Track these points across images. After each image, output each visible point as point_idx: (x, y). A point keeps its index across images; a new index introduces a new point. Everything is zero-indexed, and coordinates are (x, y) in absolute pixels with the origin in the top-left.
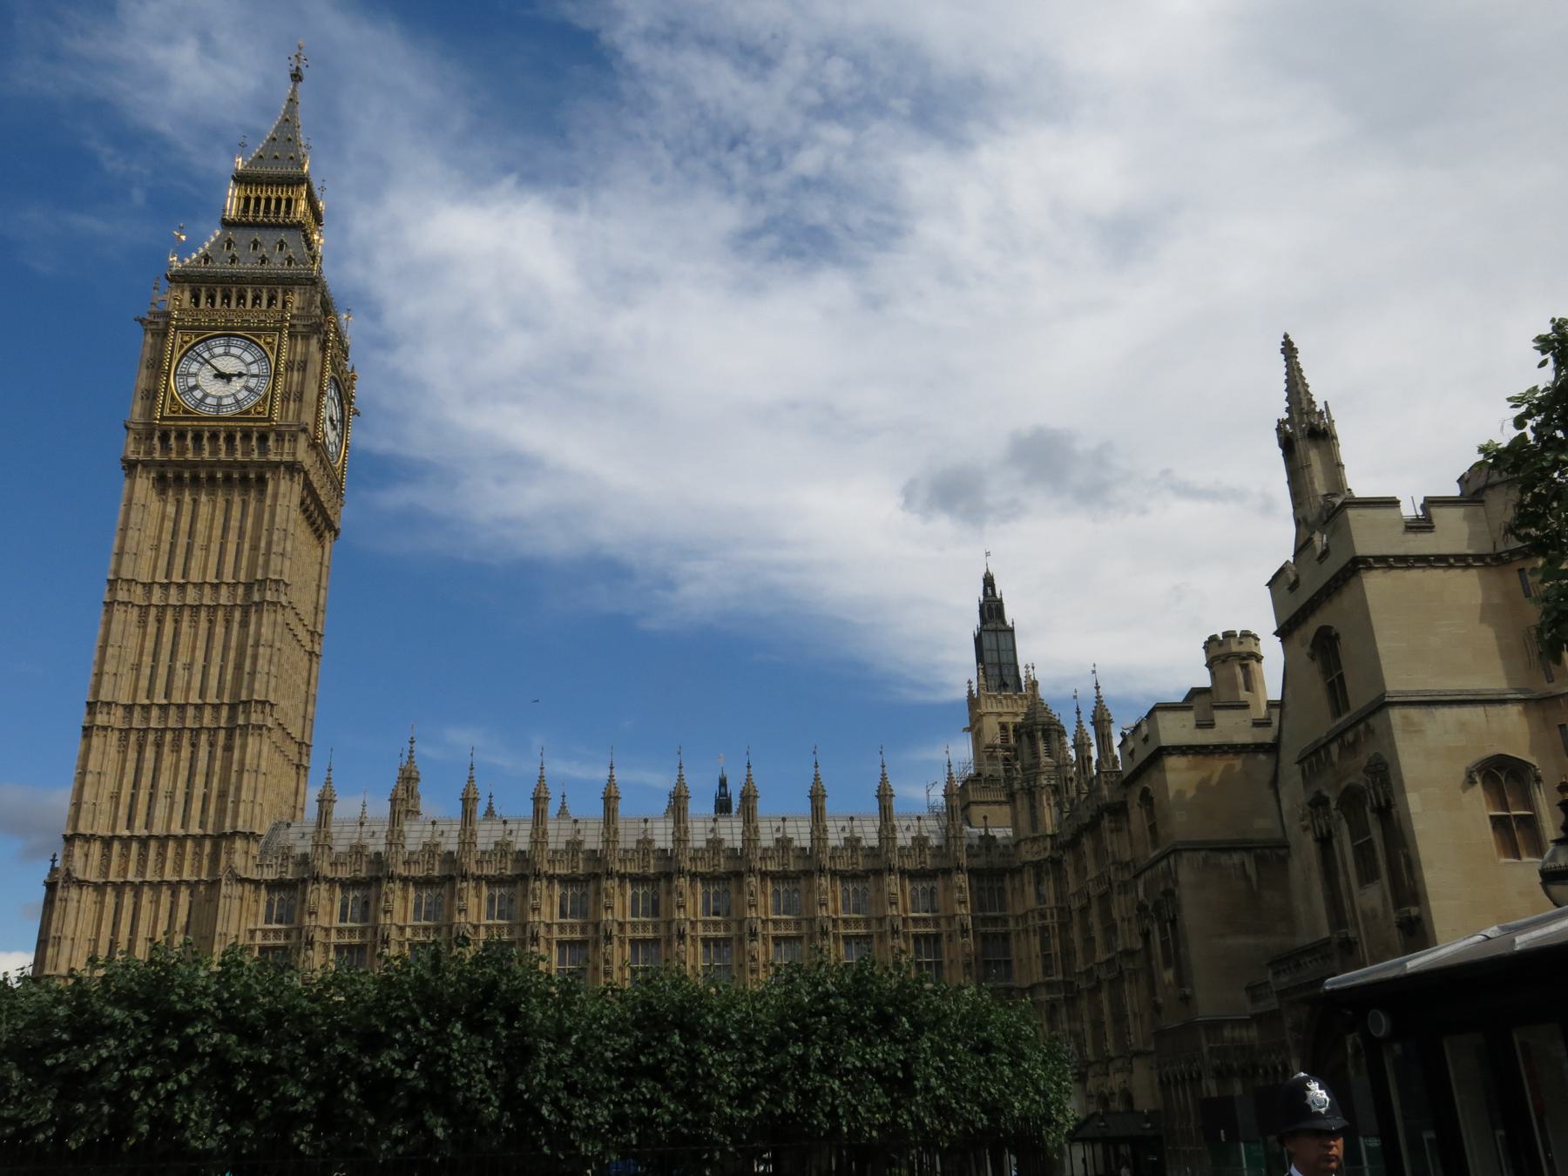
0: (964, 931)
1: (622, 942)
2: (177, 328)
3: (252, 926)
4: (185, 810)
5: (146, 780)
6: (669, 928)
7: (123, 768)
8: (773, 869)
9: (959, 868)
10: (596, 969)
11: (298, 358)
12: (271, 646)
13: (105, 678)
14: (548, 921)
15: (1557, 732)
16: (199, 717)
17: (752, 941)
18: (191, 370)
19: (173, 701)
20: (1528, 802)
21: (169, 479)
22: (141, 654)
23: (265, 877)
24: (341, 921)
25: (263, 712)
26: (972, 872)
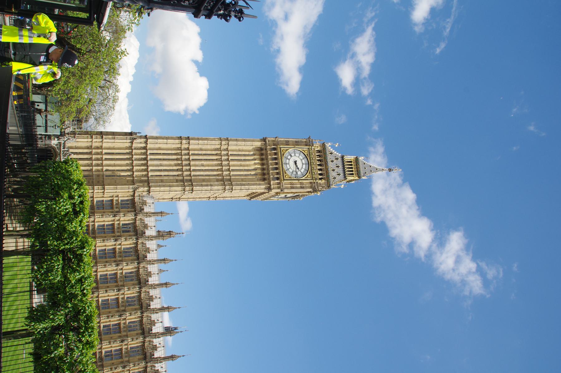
1: (119, 320)
2: (309, 148)
3: (119, 196)
8: (148, 370)
10: (110, 312)
16: (187, 170)
17: (122, 367)
18: (296, 154)
21: (261, 152)
23: (136, 198)
25: (189, 190)
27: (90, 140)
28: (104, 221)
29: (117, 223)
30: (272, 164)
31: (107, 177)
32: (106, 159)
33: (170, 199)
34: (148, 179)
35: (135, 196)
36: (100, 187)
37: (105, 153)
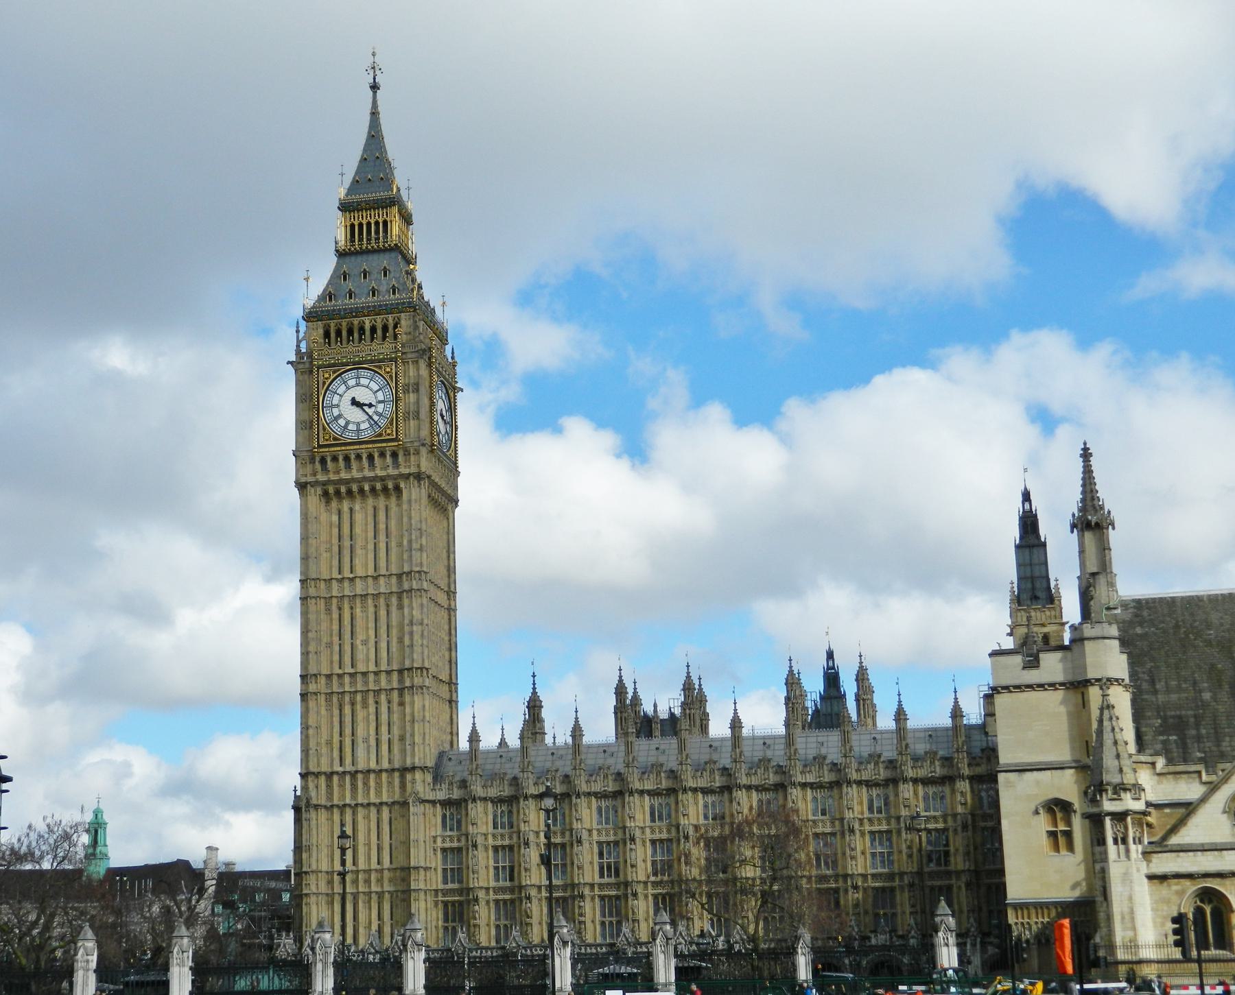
0: (965, 827)
2: (318, 369)
3: (433, 834)
4: (377, 751)
5: (348, 731)
7: (332, 722)
9: (962, 777)
12: (422, 624)
13: (311, 656)
14: (642, 825)
16: (377, 682)
18: (335, 402)
20: (1069, 823)
22: (331, 635)
23: (438, 798)
24: (494, 828)
26: (973, 779)
29: (491, 841)
30: (361, 469)
34: (398, 770)
36: (412, 878)
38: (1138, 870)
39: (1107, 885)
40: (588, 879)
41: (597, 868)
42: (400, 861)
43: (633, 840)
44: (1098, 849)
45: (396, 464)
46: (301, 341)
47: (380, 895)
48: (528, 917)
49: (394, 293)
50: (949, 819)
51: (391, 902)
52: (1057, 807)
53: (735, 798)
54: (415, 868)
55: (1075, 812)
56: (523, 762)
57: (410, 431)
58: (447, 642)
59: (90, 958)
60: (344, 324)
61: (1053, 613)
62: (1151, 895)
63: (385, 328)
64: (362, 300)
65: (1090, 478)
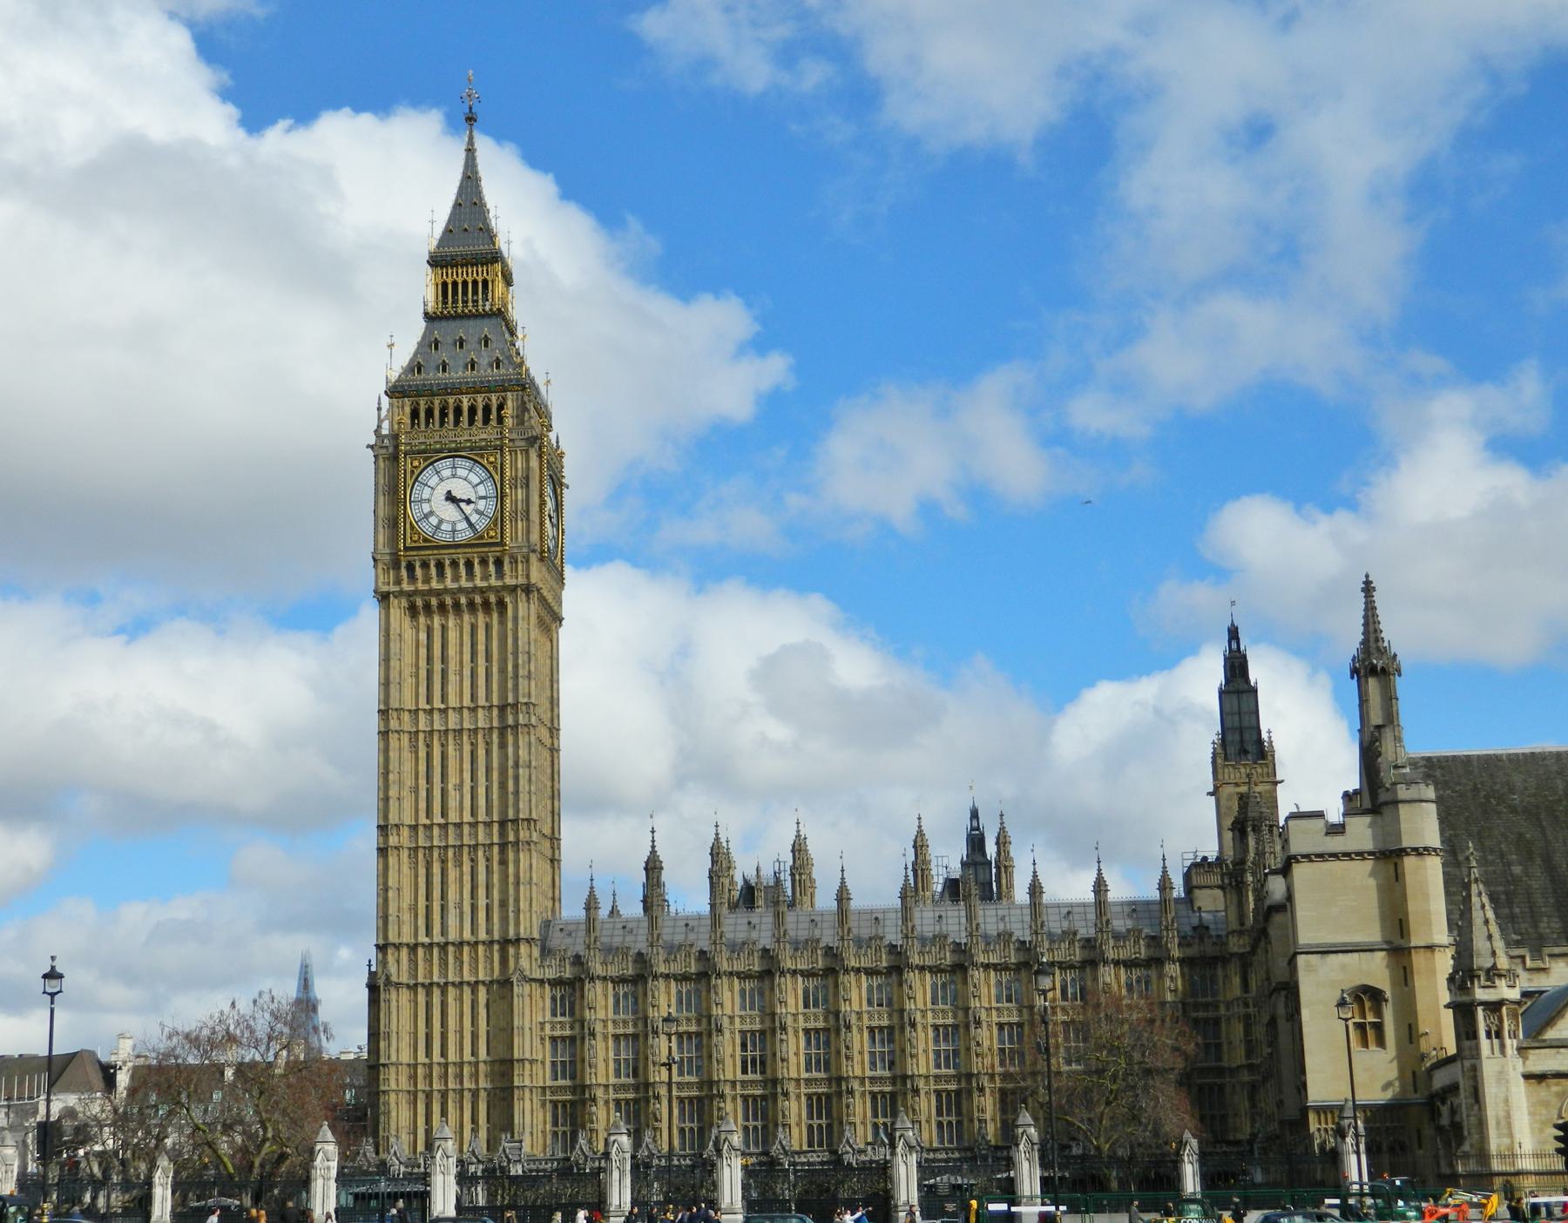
1: (860, 1030)
3: (540, 1019)
6: (902, 1017)
8: (996, 961)
9: (1172, 960)
10: (838, 1052)
11: (520, 474)
13: (391, 802)
14: (794, 1011)
15: (1402, 971)
17: (976, 1028)
18: (425, 496)
19: (450, 821)
20: (1379, 1014)
22: (417, 778)
23: (547, 976)
25: (529, 829)
26: (1182, 961)
27: (393, 1096)
28: (606, 1061)
30: (456, 578)
31: (491, 1051)
32: (444, 1054)
33: (553, 868)
34: (498, 942)
35: (541, 977)
36: (516, 1072)
37: (427, 1056)
38: (1514, 1069)
39: (1480, 1085)
40: (729, 1076)
41: (739, 1064)
42: (501, 1053)
43: (784, 1029)
44: (1467, 1043)
45: (500, 574)
46: (383, 421)
47: (475, 1094)
48: (657, 1120)
49: (498, 367)
50: (1156, 1007)
51: (488, 1102)
52: (1368, 996)
53: (906, 980)
54: (518, 1061)
55: (1386, 1001)
56: (652, 934)
57: (513, 538)
58: (549, 790)
59: (331, 1163)
60: (437, 402)
61: (1265, 770)
62: (1528, 1097)
63: (487, 410)
64: (457, 374)
65: (1373, 615)
